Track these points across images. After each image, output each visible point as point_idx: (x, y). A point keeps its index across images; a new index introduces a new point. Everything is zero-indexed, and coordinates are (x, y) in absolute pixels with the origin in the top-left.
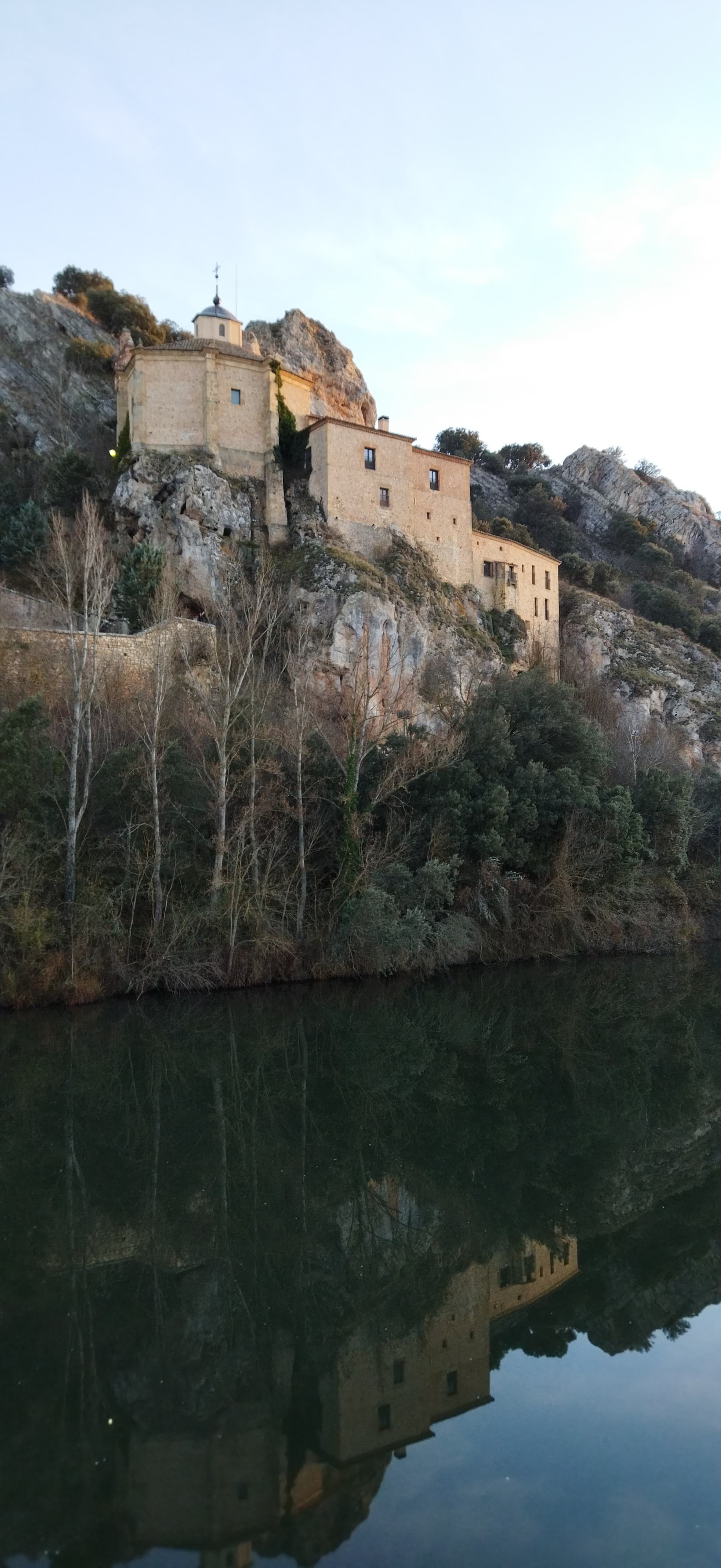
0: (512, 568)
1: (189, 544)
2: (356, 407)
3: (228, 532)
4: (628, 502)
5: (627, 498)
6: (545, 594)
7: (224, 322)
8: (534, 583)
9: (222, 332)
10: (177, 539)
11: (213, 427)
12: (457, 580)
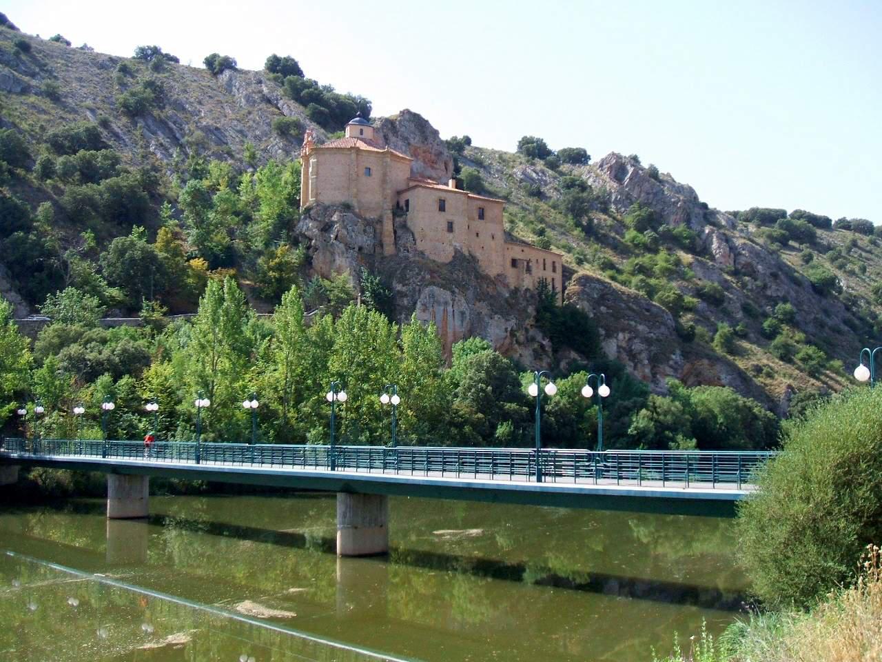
0: (528, 263)
3: (360, 249)
6: (553, 275)
7: (361, 136)
8: (544, 269)
9: (362, 131)
10: (333, 254)
12: (493, 272)
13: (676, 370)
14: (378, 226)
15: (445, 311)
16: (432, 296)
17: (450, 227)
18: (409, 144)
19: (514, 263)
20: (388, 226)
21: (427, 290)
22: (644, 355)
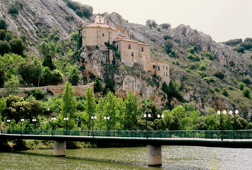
1: (95, 65)
3: (102, 62)
4: (192, 38)
5: (191, 37)
10: (92, 64)
11: (99, 42)
13: (210, 103)
15: (133, 84)
18: (115, 24)
22: (199, 98)
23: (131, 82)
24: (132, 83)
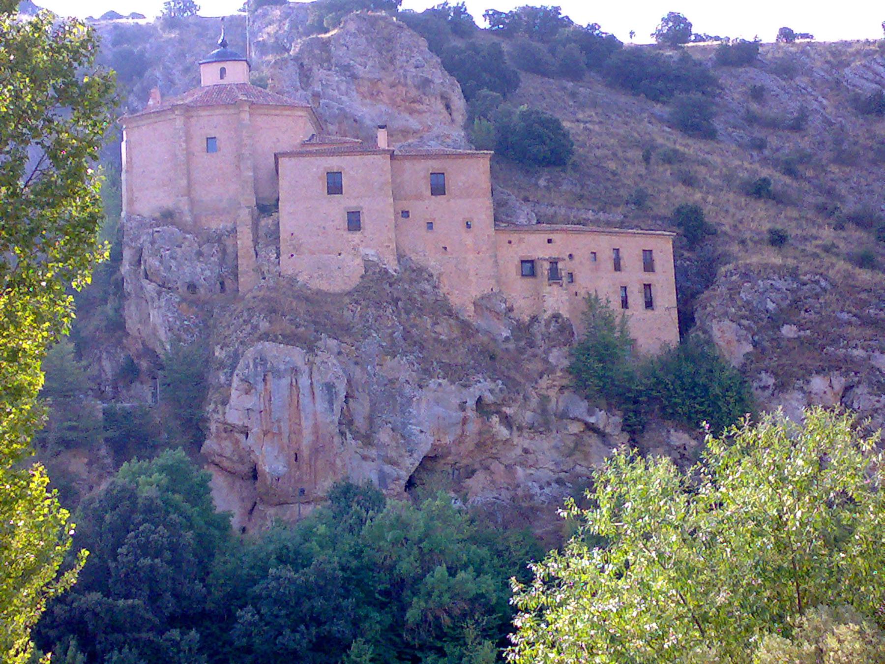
2: (433, 100)
6: (648, 277)
14: (229, 242)
15: (294, 386)
16: (261, 360)
17: (354, 221)
18: (354, 77)
19: (529, 268)
20: (245, 239)
21: (250, 353)
23: (280, 378)
24: (285, 381)
